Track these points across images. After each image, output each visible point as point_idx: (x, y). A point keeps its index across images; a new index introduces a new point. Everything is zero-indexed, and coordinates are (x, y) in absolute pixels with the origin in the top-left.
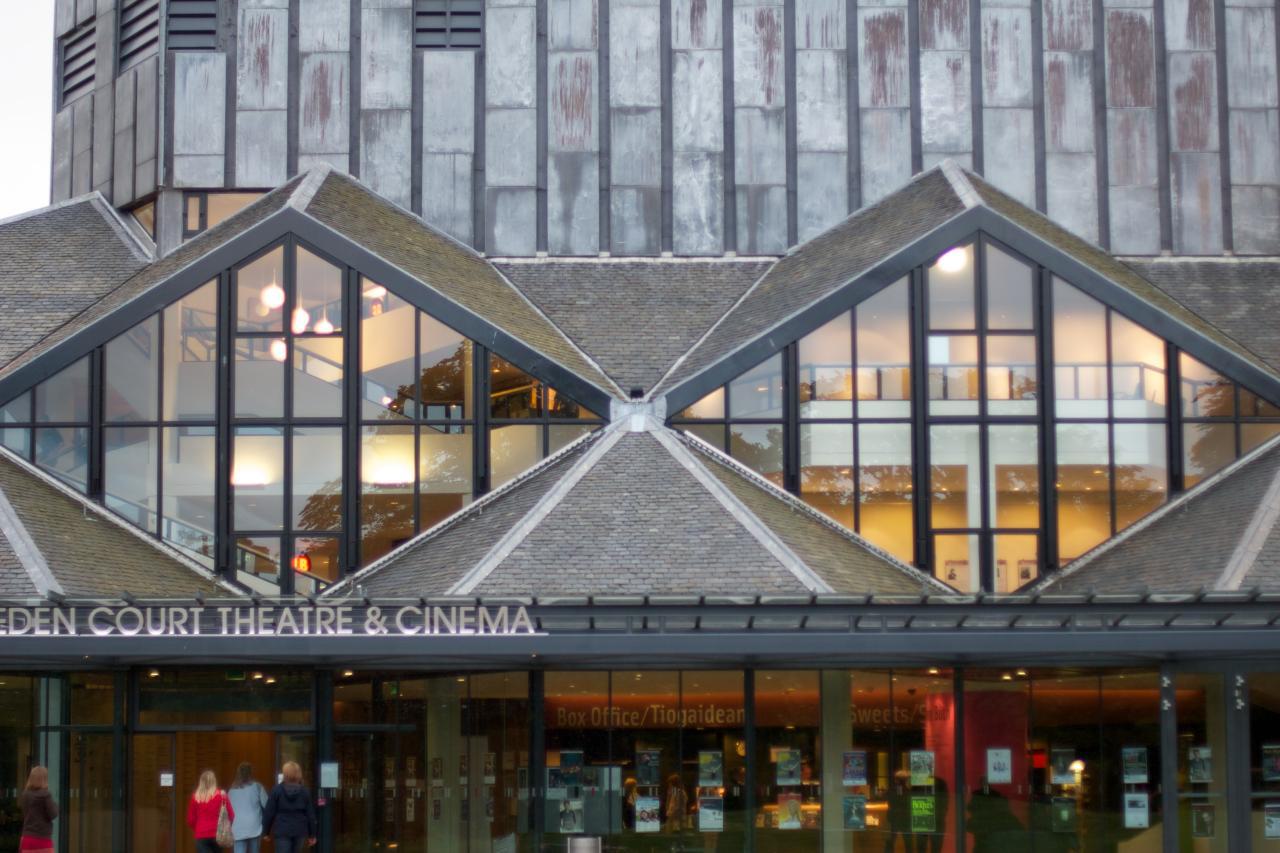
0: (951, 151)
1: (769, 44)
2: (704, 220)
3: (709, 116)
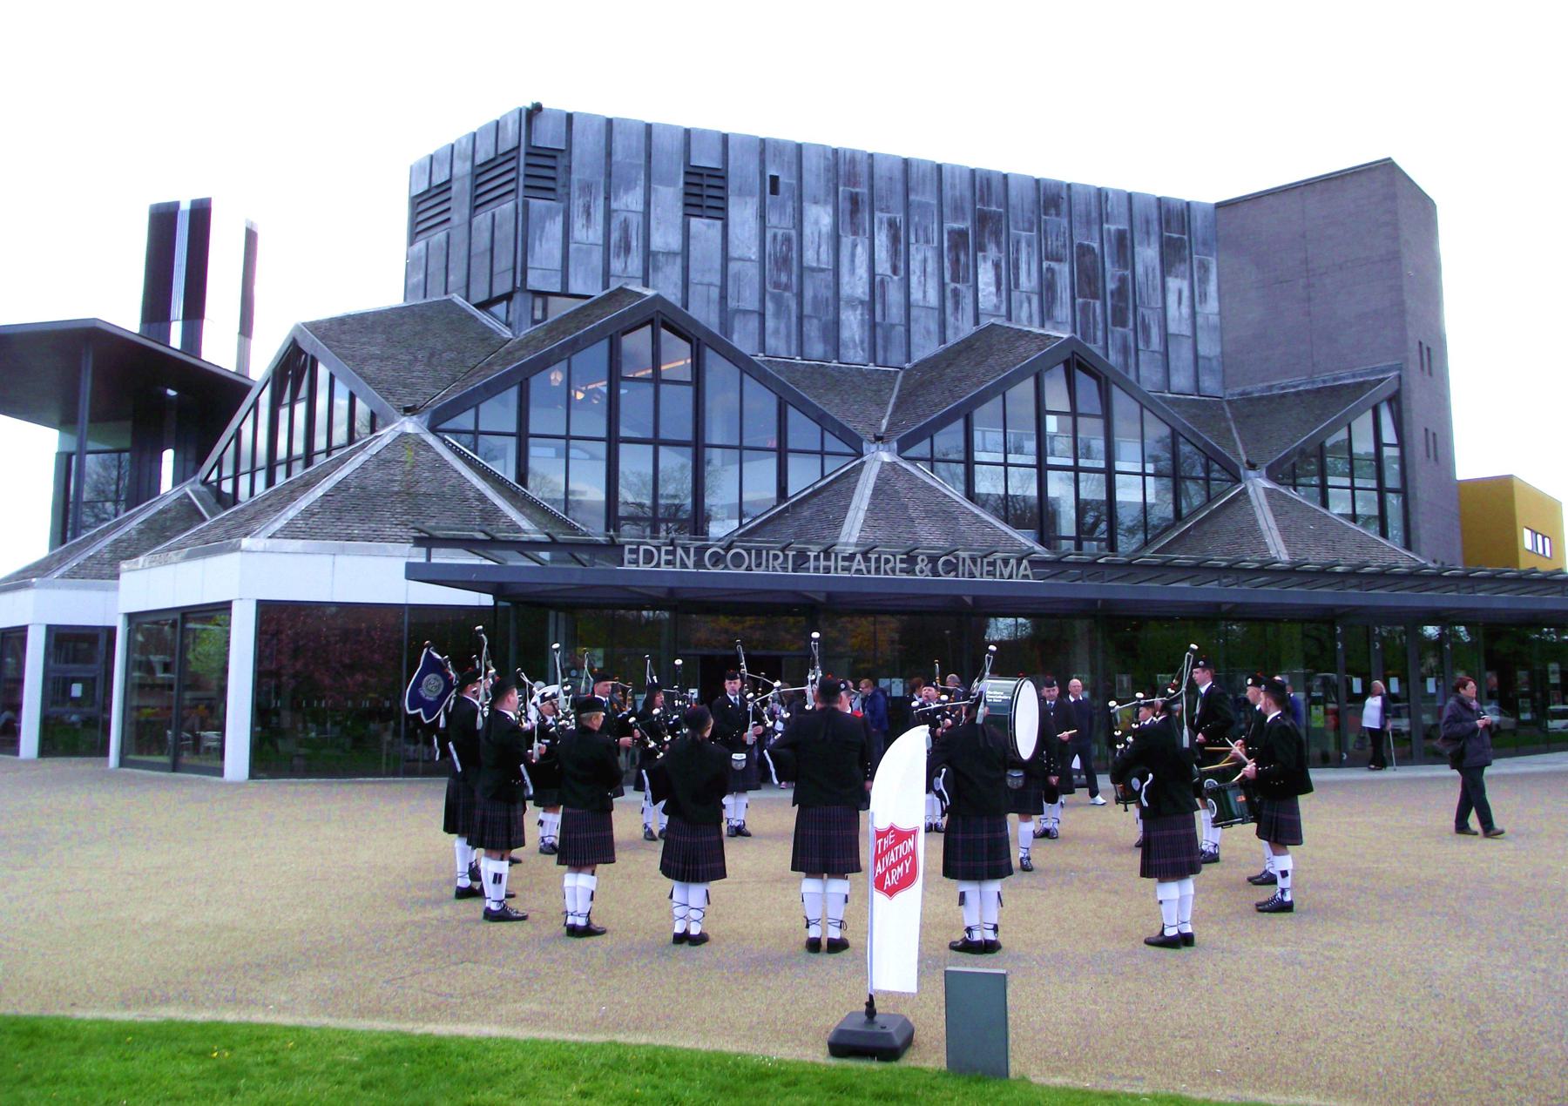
2: (857, 341)
3: (861, 278)
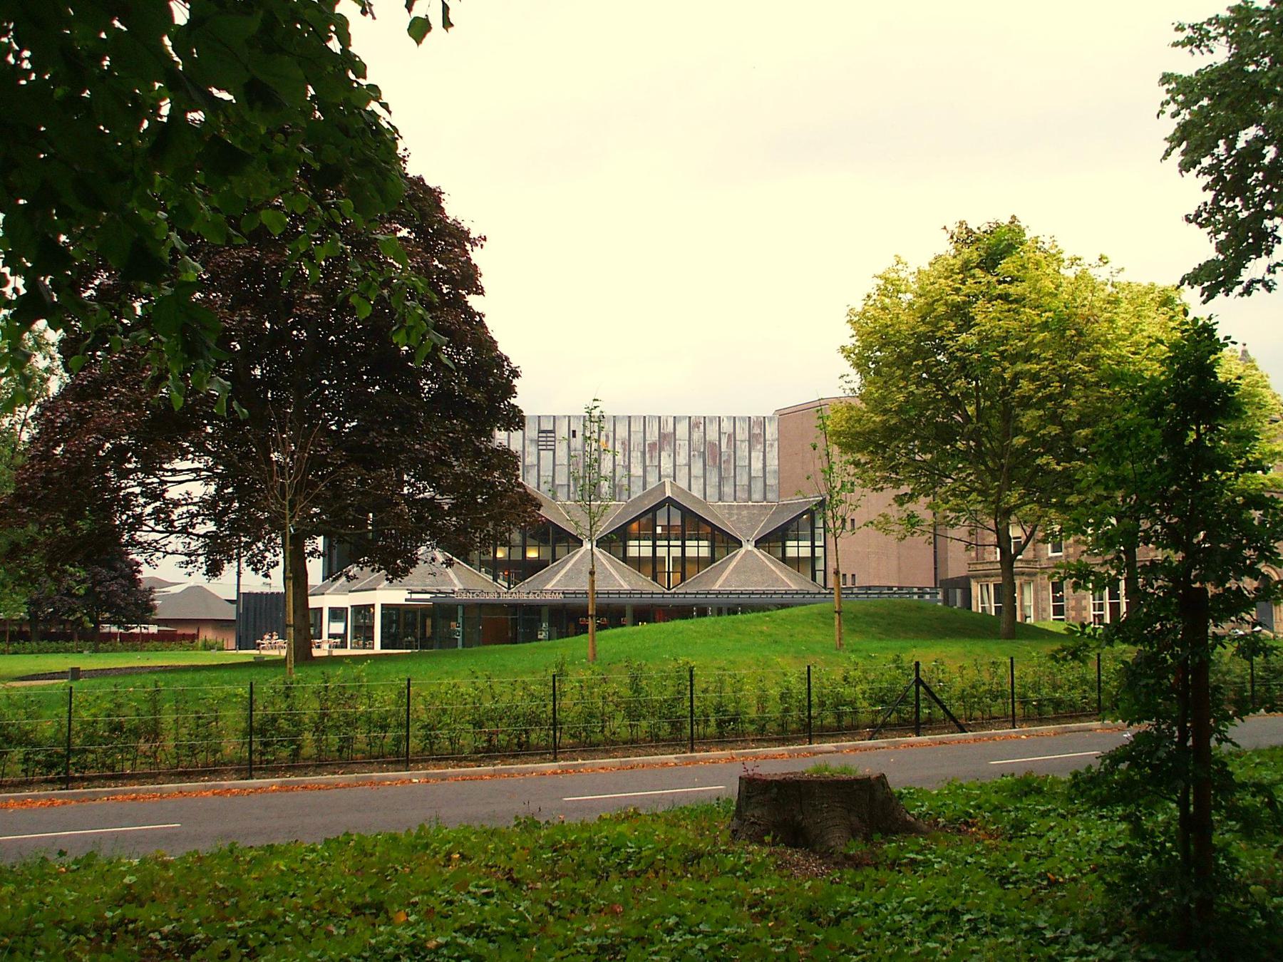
0: (668, 476)
1: (624, 450)
